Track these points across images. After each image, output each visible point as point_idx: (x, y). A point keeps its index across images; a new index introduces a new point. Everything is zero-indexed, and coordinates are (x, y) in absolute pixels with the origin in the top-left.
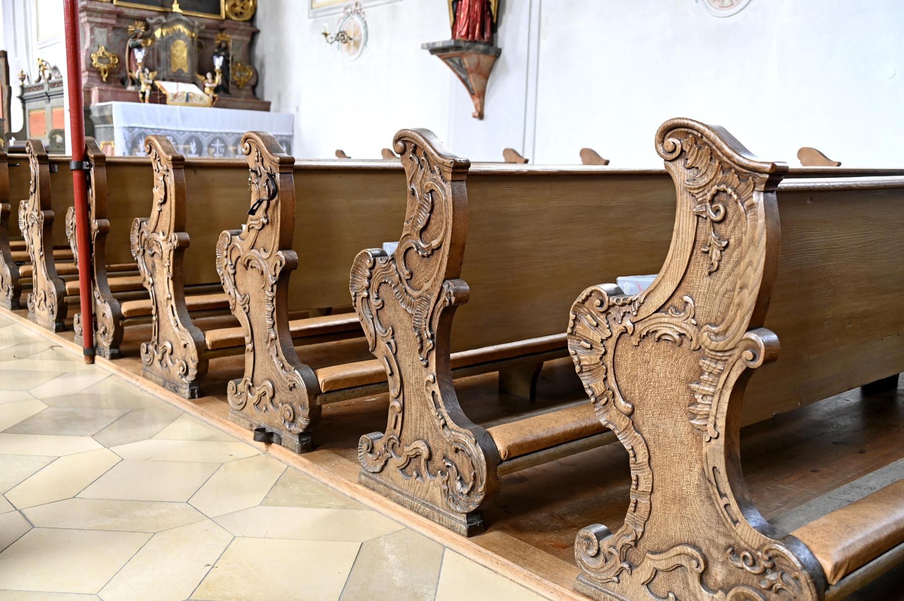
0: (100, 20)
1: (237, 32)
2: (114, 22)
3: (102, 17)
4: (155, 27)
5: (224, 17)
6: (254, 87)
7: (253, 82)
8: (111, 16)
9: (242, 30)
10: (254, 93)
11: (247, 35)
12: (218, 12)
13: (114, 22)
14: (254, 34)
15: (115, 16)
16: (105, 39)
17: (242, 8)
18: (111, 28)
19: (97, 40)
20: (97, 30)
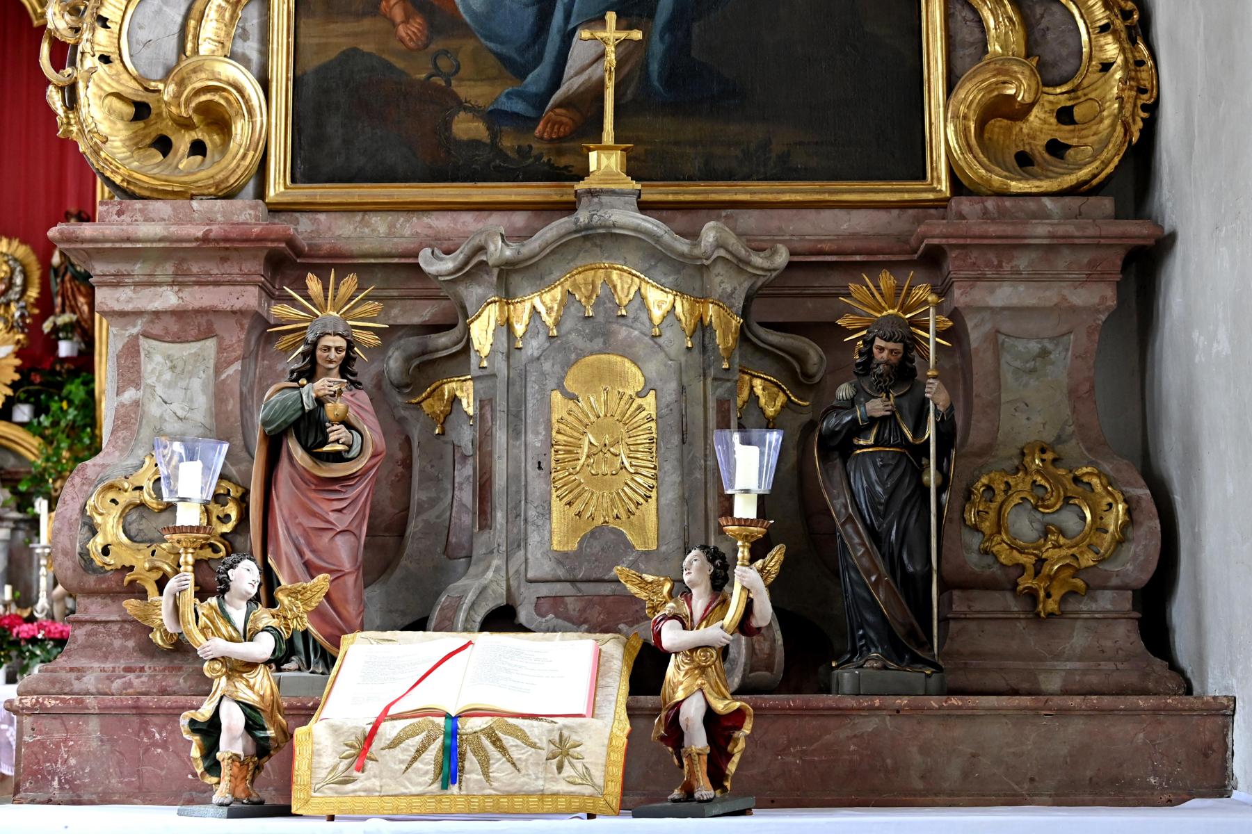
0: (169, 299)
1: (1023, 261)
2: (250, 298)
3: (178, 283)
4: (471, 293)
5: (944, 186)
6: (1153, 602)
7: (1137, 563)
8: (232, 269)
9: (1052, 248)
10: (1155, 632)
11: (1093, 275)
12: (918, 172)
13: (250, 298)
14: (1143, 266)
15: (255, 266)
16: (202, 402)
17: (1065, 116)
18: (235, 336)
19: (154, 409)
20: (157, 358)
